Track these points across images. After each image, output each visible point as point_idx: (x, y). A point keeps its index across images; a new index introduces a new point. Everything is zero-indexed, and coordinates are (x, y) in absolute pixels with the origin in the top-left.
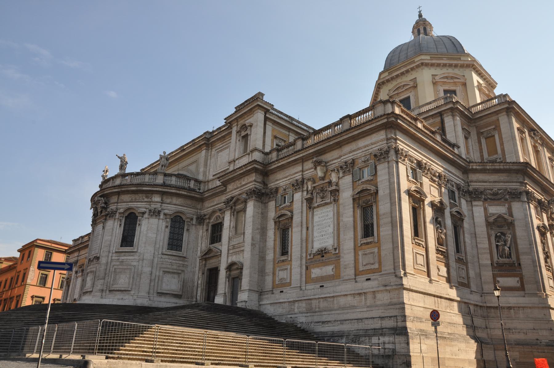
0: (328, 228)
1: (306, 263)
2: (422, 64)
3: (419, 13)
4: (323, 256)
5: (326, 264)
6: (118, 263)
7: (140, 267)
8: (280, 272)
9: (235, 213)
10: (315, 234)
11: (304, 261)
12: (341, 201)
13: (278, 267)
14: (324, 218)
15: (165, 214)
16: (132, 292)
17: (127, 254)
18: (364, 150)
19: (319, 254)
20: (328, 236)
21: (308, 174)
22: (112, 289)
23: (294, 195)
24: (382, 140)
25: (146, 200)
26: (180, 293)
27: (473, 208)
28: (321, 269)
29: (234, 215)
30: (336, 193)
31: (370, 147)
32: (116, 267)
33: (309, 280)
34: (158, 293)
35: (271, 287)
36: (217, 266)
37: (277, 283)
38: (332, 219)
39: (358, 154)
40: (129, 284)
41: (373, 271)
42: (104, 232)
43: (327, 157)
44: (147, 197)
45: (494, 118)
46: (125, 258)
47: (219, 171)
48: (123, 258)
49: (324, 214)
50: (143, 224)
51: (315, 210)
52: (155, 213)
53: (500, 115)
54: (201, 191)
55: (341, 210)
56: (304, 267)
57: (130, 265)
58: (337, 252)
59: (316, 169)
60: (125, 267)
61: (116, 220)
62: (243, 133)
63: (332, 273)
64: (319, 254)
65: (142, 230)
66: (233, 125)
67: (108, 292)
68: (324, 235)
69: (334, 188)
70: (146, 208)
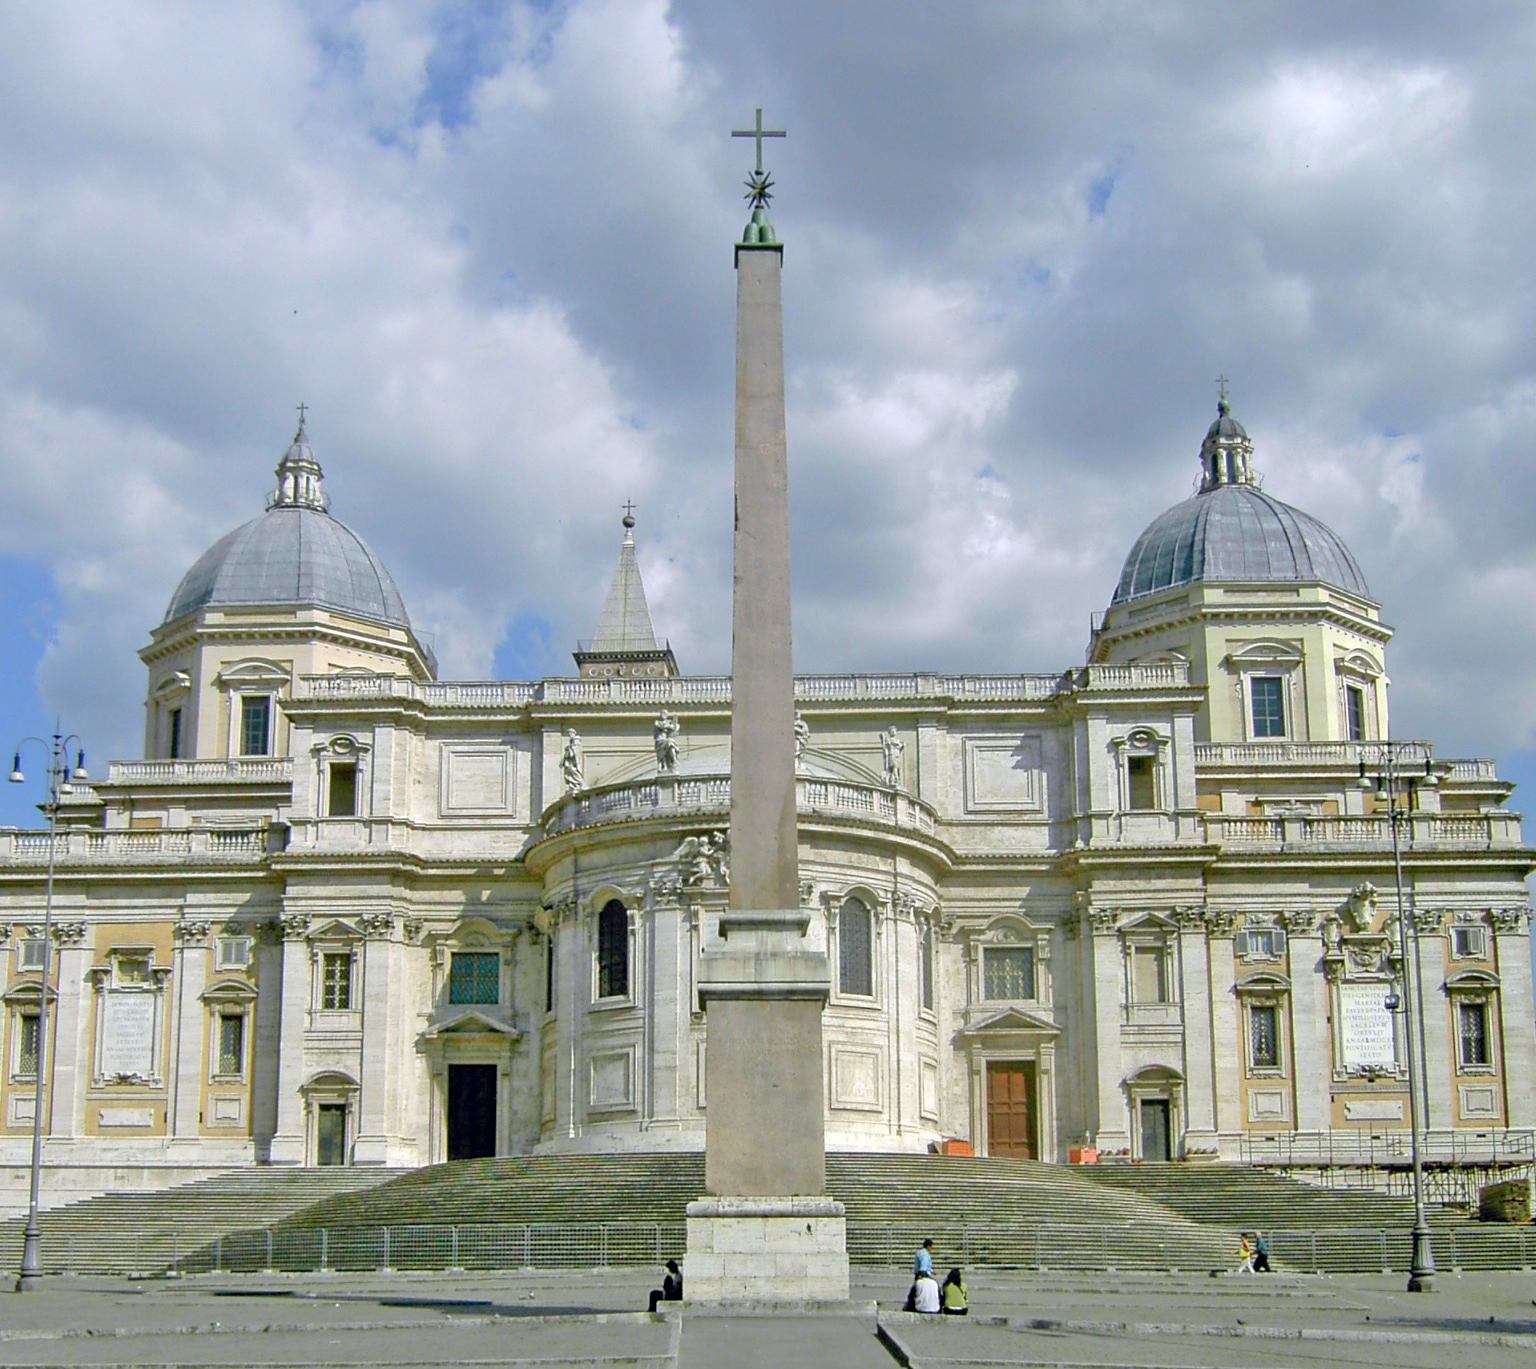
0: (1381, 1028)
1: (1331, 1087)
3: (1219, 399)
4: (1371, 1080)
6: (842, 1038)
9: (1133, 948)
11: (1324, 1085)
12: (1414, 983)
13: (1252, 1086)
14: (1370, 1007)
15: (918, 913)
16: (885, 1116)
17: (861, 1012)
18: (1469, 898)
19: (1363, 1077)
20: (1382, 1044)
23: (1290, 941)
25: (882, 868)
28: (1371, 1105)
32: (840, 1047)
33: (1341, 1119)
34: (922, 1118)
35: (1239, 1126)
39: (1458, 901)
40: (877, 1095)
41: (1491, 1122)
46: (859, 1023)
48: (854, 1023)
49: (1369, 999)
50: (884, 936)
60: (864, 1050)
63: (1401, 1116)
64: (1363, 1077)
65: (884, 951)
68: (1373, 1040)
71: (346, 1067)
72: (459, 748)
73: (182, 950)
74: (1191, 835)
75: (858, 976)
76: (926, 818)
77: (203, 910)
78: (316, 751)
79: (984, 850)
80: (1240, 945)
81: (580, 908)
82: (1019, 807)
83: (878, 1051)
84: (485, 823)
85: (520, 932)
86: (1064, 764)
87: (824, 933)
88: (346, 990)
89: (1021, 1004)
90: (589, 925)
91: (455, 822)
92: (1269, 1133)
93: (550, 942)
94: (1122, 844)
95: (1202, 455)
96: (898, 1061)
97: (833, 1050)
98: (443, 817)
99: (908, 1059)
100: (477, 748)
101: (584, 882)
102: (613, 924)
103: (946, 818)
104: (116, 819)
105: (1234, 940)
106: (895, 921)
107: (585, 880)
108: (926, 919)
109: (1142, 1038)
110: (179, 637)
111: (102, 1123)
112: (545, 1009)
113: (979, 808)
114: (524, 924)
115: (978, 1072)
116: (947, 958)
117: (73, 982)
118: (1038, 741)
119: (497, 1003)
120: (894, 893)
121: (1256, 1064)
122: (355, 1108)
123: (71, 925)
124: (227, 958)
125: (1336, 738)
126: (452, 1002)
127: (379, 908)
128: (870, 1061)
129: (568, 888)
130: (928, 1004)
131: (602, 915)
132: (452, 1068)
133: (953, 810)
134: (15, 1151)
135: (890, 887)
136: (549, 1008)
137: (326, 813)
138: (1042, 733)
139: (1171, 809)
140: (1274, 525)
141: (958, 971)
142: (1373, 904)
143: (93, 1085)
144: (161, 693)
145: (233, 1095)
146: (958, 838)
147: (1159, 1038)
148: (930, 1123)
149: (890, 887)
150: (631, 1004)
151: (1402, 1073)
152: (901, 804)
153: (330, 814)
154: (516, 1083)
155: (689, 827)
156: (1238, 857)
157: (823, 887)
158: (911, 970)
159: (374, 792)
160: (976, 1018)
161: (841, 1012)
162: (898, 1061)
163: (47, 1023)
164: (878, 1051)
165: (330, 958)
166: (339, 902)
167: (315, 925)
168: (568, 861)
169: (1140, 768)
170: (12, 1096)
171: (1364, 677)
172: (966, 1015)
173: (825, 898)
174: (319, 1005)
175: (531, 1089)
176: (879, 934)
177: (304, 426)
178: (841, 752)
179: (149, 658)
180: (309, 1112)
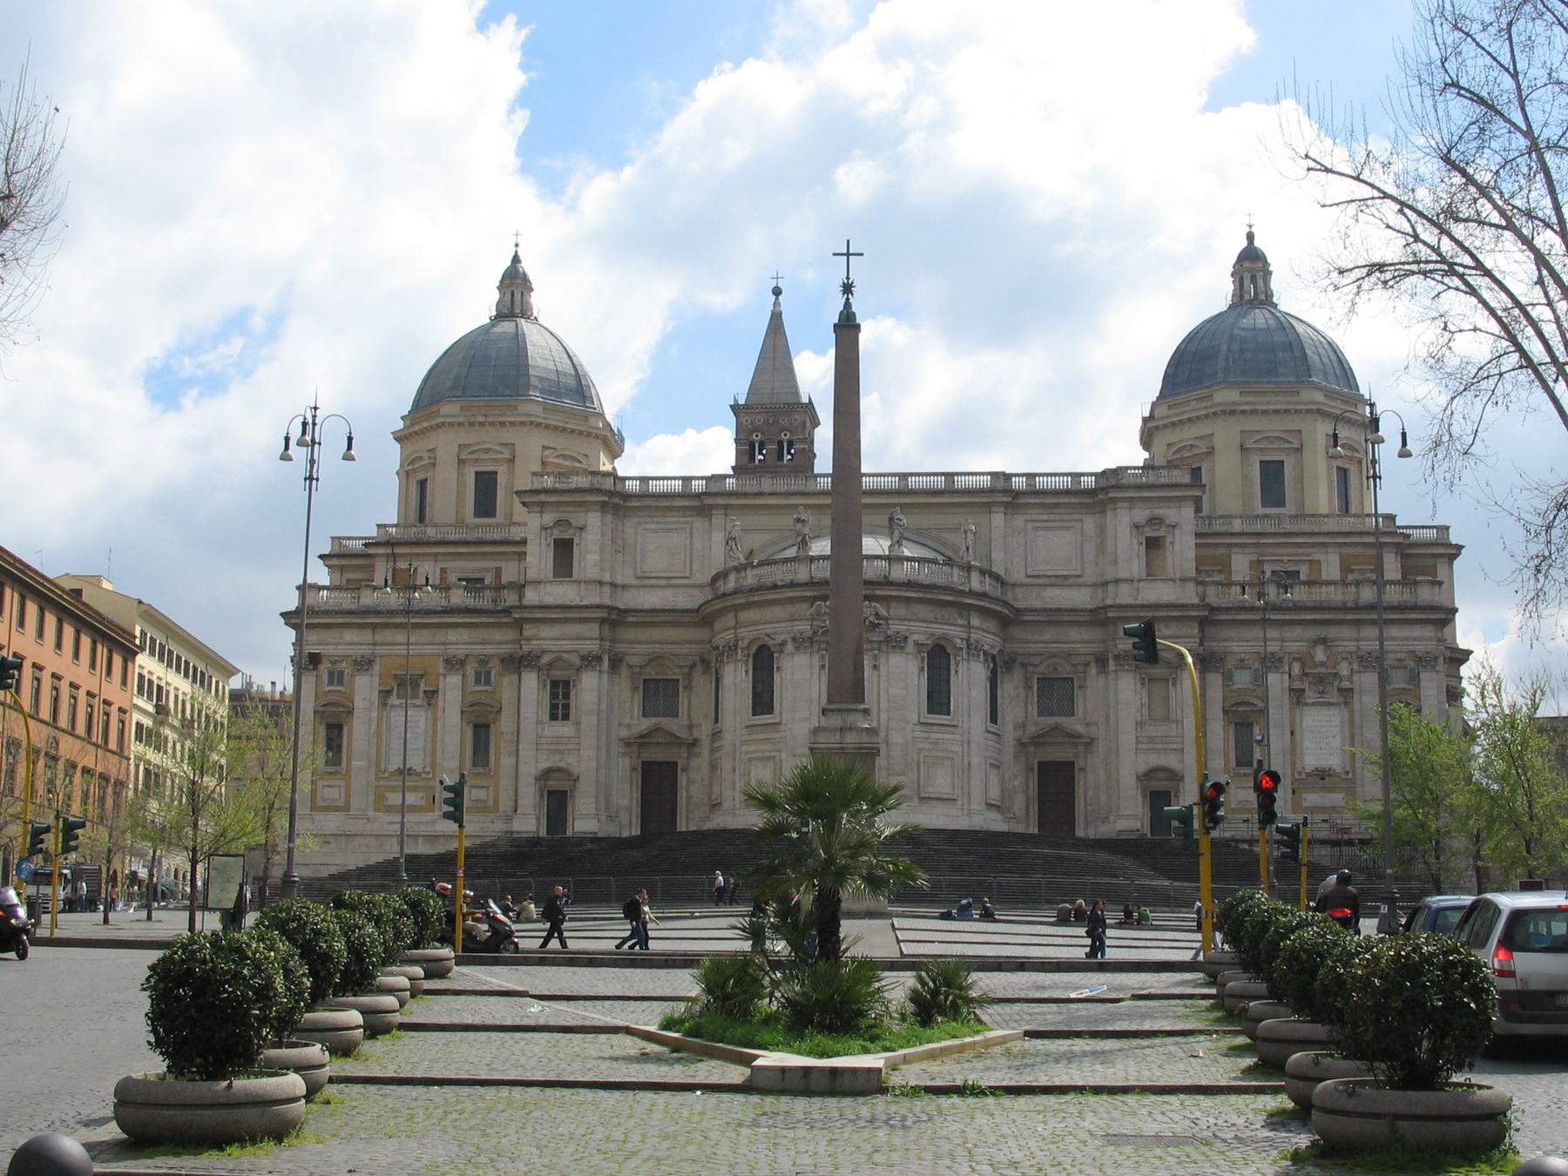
1: (1292, 783)
2: (1318, 411)
3: (1248, 230)
5: (1330, 790)
6: (928, 746)
7: (965, 757)
8: (1239, 791)
10: (1307, 744)
12: (1357, 706)
15: (985, 653)
16: (960, 803)
21: (1292, 647)
22: (926, 795)
24: (1430, 639)
26: (999, 804)
27: (1088, 589)
29: (1143, 684)
30: (1346, 693)
31: (1410, 643)
32: (927, 753)
34: (989, 805)
36: (1072, 759)
37: (1233, 806)
38: (1338, 729)
40: (953, 787)
42: (879, 676)
43: (1332, 632)
44: (961, 616)
45: (1430, 562)
47: (1048, 573)
48: (932, 735)
51: (1305, 708)
52: (972, 648)
53: (1438, 560)
54: (1020, 605)
55: (1357, 716)
56: (1291, 792)
57: (953, 752)
58: (1350, 776)
59: (1313, 647)
60: (944, 755)
61: (910, 657)
62: (1149, 532)
66: (1119, 505)
67: (916, 799)
69: (1345, 684)
70: (962, 639)
71: (567, 763)
72: (649, 526)
73: (445, 675)
74: (1190, 595)
75: (938, 699)
76: (994, 583)
77: (459, 647)
78: (544, 528)
79: (1038, 604)
80: (1228, 678)
81: (739, 651)
82: (1065, 573)
83: (955, 756)
84: (669, 582)
85: (694, 665)
86: (1099, 541)
87: (916, 671)
88: (567, 707)
89: (1062, 720)
90: (746, 663)
91: (646, 582)
92: (1245, 817)
93: (717, 673)
94: (1139, 602)
95: (1232, 275)
96: (969, 764)
97: (922, 756)
98: (638, 578)
99: (976, 760)
100: (661, 526)
101: (742, 632)
102: (764, 662)
103: (1011, 581)
104: (381, 572)
105: (1223, 673)
106: (968, 660)
107: (742, 630)
108: (994, 658)
109: (1151, 746)
110: (425, 424)
111: (388, 803)
112: (713, 721)
113: (1035, 573)
114: (697, 658)
115: (1032, 769)
116: (1010, 687)
117: (365, 699)
118: (1080, 524)
119: (677, 716)
120: (968, 640)
121: (1238, 765)
122: (577, 794)
123: (363, 656)
124: (478, 682)
125: (1324, 510)
126: (644, 715)
127: (593, 647)
128: (948, 763)
129: (730, 635)
130: (994, 720)
131: (755, 655)
132: (644, 763)
133: (1018, 575)
134: (323, 823)
135: (964, 635)
136: (716, 721)
137: (550, 575)
138: (1084, 517)
139: (1177, 576)
140: (1283, 339)
141: (1018, 695)
142: (1328, 647)
143: (380, 775)
144: (410, 467)
145: (484, 783)
146: (1020, 596)
147: (1165, 746)
148: (994, 808)
149: (964, 635)
150: (778, 721)
151: (1347, 773)
152: (975, 575)
153: (554, 577)
154: (693, 775)
155: (815, 593)
156: (1228, 610)
157: (916, 637)
158: (980, 696)
159: (590, 557)
160: (1031, 729)
161: (928, 728)
162: (969, 764)
163: (345, 730)
164: (955, 756)
165: (554, 684)
166: (563, 642)
167: (546, 659)
168: (731, 616)
169: (1153, 544)
170: (320, 783)
171: (1351, 458)
172: (1024, 725)
173: (917, 644)
174: (546, 717)
175: (702, 780)
176: (956, 671)
177: (519, 250)
178: (934, 531)
179: (400, 437)
180: (542, 796)
